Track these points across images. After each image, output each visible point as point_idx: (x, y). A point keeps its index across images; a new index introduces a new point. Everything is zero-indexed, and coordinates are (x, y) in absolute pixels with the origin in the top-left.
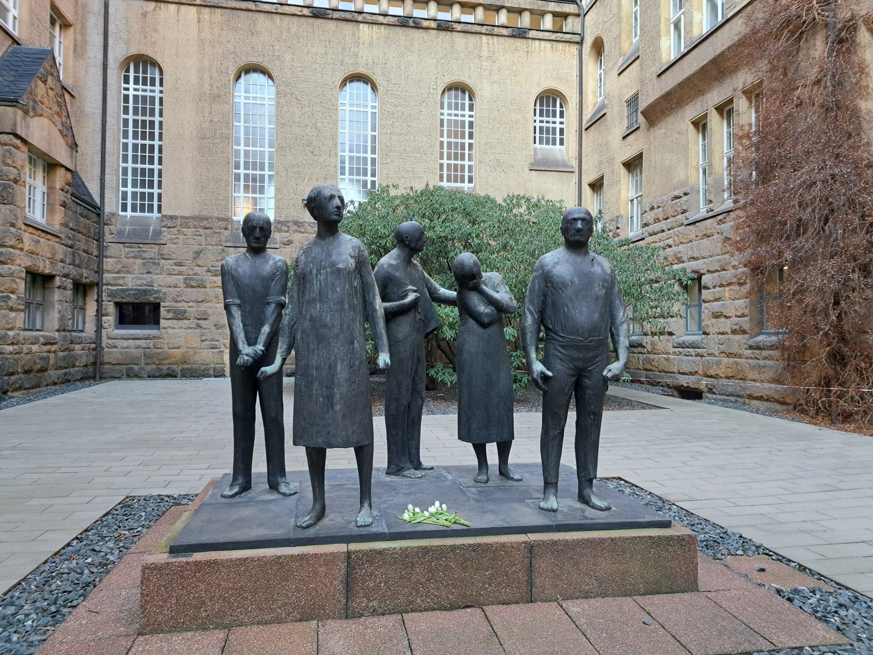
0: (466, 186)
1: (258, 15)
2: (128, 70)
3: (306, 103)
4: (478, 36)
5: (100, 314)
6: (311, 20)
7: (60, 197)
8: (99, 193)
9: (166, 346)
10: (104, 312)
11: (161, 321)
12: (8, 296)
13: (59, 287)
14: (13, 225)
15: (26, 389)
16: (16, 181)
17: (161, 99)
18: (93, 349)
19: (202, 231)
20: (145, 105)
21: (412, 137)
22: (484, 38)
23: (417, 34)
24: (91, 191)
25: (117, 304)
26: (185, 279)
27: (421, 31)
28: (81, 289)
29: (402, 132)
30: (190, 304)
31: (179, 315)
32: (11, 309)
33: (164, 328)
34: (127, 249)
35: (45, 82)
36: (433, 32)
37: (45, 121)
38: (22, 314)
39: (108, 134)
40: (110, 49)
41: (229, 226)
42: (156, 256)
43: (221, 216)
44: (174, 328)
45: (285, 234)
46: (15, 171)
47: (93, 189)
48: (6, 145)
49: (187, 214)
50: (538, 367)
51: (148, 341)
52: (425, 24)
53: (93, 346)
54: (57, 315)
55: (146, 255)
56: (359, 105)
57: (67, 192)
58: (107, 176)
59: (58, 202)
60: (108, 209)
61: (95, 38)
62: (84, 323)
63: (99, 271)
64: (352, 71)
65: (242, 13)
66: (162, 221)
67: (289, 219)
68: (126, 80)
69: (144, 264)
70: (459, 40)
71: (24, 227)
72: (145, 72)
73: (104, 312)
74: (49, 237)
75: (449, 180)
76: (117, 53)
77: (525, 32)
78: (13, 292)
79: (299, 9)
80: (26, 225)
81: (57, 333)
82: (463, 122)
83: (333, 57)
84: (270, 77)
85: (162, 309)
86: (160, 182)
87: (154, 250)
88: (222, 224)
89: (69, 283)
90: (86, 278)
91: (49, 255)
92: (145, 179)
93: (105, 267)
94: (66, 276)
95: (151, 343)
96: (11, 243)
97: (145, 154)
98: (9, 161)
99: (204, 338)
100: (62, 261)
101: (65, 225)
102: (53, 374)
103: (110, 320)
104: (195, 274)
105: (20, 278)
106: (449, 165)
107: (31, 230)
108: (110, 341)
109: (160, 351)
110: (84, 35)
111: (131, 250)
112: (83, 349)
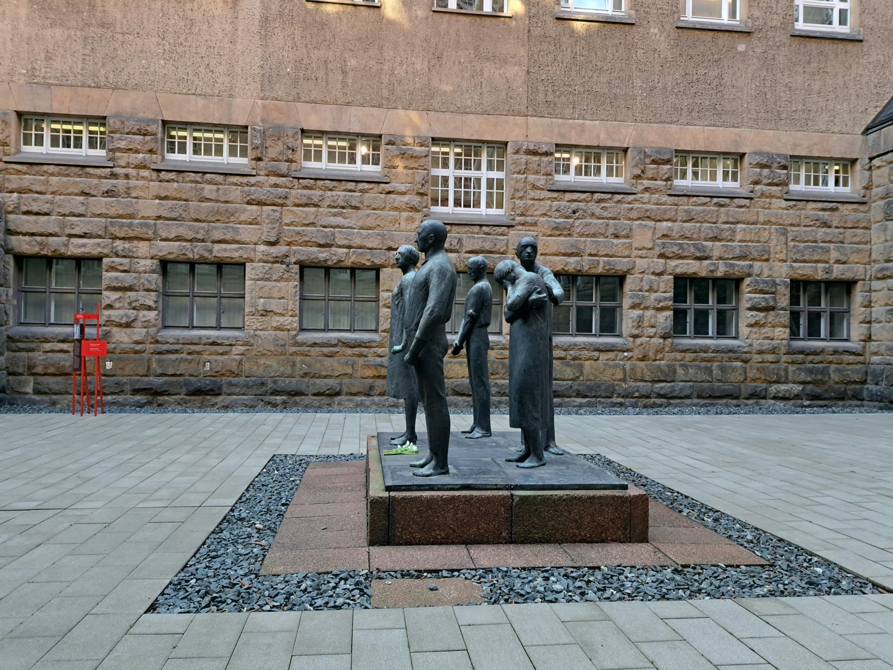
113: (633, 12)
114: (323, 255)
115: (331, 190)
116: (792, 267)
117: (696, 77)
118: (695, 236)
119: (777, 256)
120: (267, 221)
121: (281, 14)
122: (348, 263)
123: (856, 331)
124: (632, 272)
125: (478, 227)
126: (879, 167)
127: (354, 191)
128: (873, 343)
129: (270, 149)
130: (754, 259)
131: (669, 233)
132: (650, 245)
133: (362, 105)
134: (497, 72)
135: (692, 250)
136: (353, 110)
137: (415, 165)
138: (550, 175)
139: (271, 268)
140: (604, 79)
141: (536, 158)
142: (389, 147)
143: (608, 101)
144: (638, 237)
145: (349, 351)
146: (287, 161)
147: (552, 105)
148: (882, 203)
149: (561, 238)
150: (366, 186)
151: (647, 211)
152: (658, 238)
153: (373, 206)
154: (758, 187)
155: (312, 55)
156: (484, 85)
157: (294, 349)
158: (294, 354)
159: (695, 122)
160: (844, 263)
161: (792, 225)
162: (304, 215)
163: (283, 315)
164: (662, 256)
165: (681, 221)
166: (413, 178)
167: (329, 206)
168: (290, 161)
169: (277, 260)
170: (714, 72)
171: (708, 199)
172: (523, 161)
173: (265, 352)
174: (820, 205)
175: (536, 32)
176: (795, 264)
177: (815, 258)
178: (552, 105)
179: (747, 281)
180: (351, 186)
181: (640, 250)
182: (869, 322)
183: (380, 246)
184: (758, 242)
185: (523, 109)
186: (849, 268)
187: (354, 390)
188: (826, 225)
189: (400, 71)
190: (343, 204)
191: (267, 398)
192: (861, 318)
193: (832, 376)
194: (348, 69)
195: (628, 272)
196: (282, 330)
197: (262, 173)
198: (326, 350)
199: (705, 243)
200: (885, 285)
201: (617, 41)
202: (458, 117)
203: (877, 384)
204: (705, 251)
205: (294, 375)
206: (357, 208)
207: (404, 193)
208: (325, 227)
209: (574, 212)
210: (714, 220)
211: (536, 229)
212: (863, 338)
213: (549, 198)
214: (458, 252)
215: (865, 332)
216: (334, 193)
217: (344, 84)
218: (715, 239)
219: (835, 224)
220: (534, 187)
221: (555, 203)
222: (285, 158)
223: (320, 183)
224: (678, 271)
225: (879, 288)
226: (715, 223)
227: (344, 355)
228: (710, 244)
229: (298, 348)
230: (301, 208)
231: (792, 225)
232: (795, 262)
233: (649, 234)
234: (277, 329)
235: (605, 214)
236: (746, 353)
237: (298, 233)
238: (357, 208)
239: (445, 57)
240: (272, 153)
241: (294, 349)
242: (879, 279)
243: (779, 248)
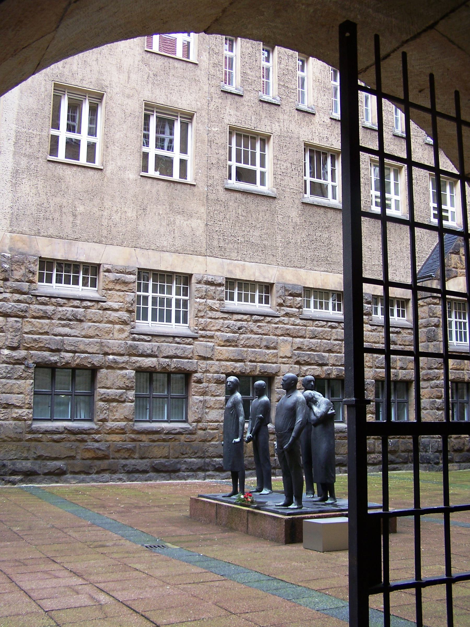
12: (435, 401)
15: (457, 462)
48: (430, 304)
50: (275, 443)
96: (435, 366)
113: (275, 189)
114: (54, 358)
115: (61, 306)
116: (375, 371)
117: (315, 237)
118: (317, 349)
120: (11, 330)
121: (28, 168)
122: (73, 365)
124: (279, 374)
125: (172, 338)
126: (422, 306)
127: (79, 307)
129: (15, 272)
131: (302, 346)
132: (289, 355)
133: (87, 241)
134: (185, 223)
135: (316, 359)
136: (80, 244)
137: (126, 289)
138: (223, 300)
139: (12, 369)
140: (257, 233)
141: (213, 288)
142: (107, 274)
143: (260, 249)
144: (282, 349)
145: (73, 437)
146: (27, 282)
147: (223, 250)
149: (231, 348)
150: (89, 304)
151: (287, 329)
152: (295, 350)
153: (94, 319)
155: (50, 201)
156: (176, 231)
157: (29, 436)
158: (30, 440)
159: (315, 268)
160: (405, 369)
162: (40, 326)
163: (20, 407)
164: (298, 363)
165: (309, 338)
166: (124, 299)
167: (60, 319)
168: (31, 282)
169: (19, 362)
170: (326, 235)
171: (325, 323)
172: (204, 289)
173: (6, 438)
175: (212, 197)
178: (223, 250)
180: (77, 303)
181: (283, 358)
183: (98, 352)
185: (203, 250)
186: (408, 372)
187: (77, 470)
189: (116, 217)
190: (71, 317)
191: (8, 478)
193: (400, 447)
194: (77, 213)
195: (276, 374)
196: (20, 420)
197: (8, 291)
198: (56, 437)
199: (324, 354)
200: (429, 385)
201: (265, 208)
202: (157, 254)
204: (324, 360)
205: (29, 457)
206: (81, 321)
207: (117, 310)
208: (56, 335)
209: (239, 329)
210: (329, 338)
211: (213, 340)
213: (222, 318)
214: (156, 356)
216: (64, 308)
217: (74, 225)
218: (330, 351)
219: (399, 342)
220: (212, 309)
221: (226, 322)
222: (26, 279)
223: (53, 300)
225: (425, 386)
226: (329, 340)
227: (69, 441)
228: (326, 354)
229: (33, 436)
230: (37, 320)
232: (377, 368)
233: (289, 347)
234: (15, 419)
235: (260, 331)
237: (35, 340)
238: (81, 321)
239: (148, 209)
240: (17, 275)
241: (29, 436)
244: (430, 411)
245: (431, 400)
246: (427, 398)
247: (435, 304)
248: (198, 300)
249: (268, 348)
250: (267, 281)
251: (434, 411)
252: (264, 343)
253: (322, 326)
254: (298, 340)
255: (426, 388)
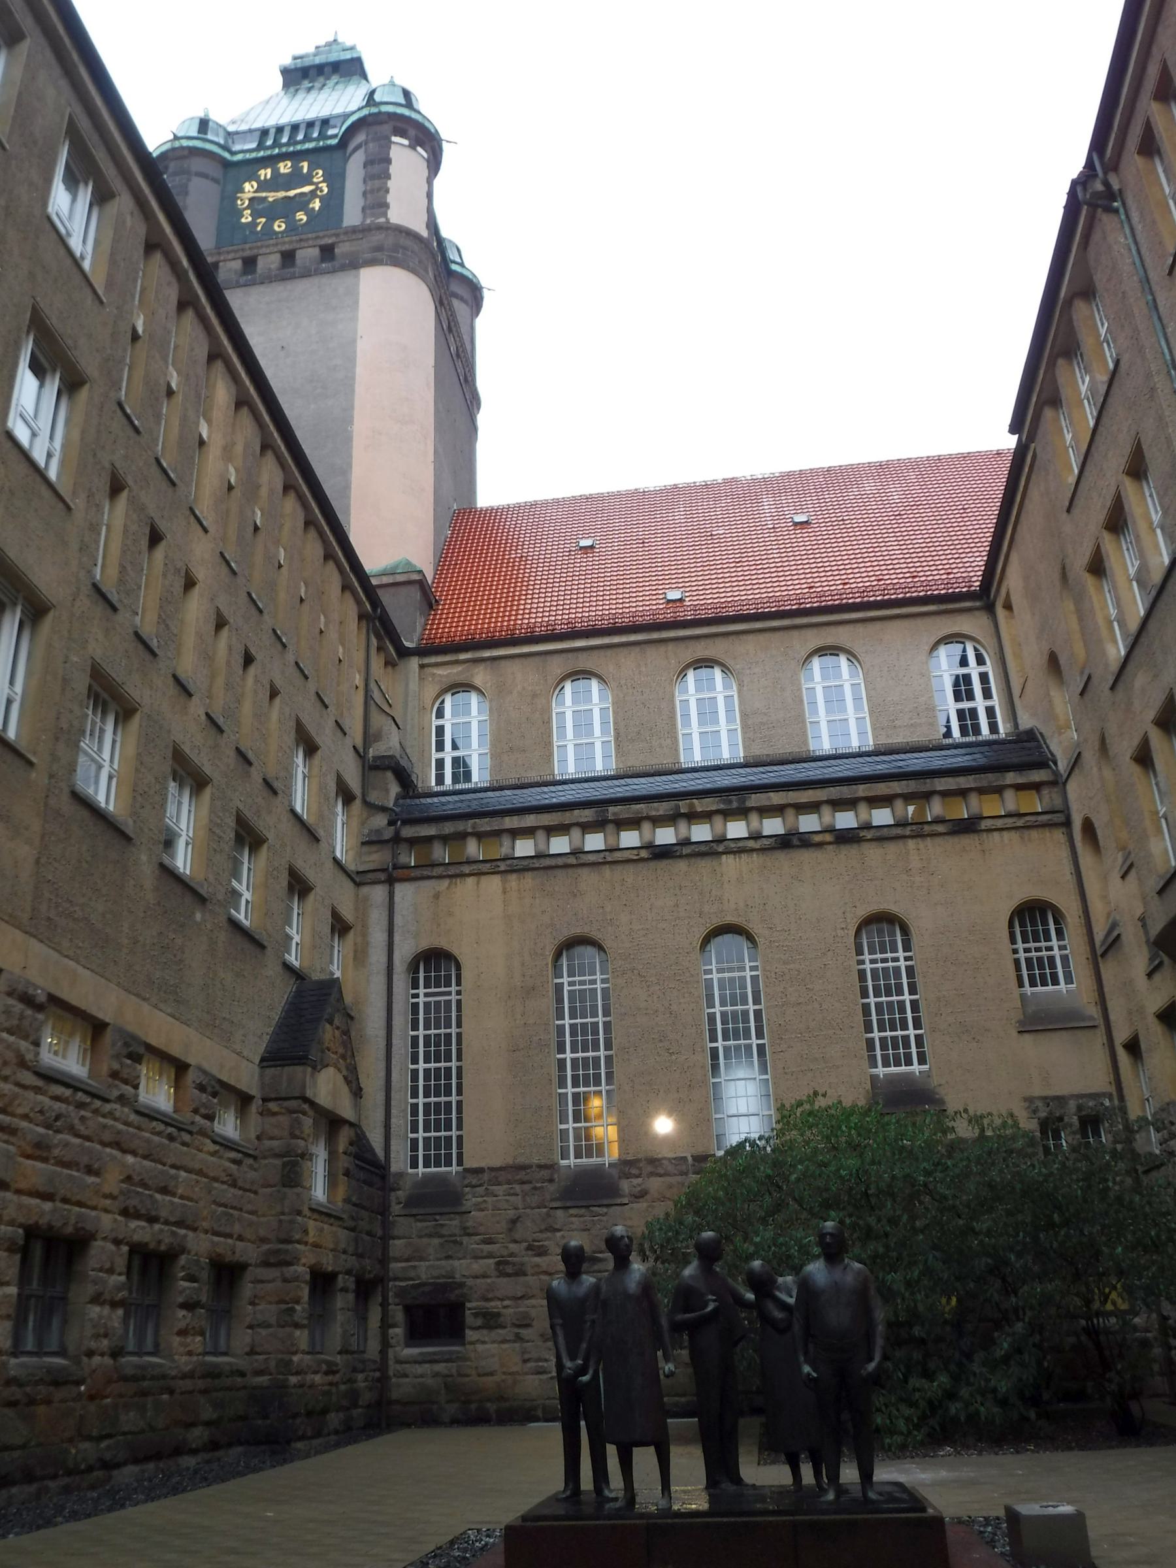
0: (916, 1068)
1: (580, 871)
2: (417, 971)
3: (653, 979)
4: (900, 843)
5: (385, 1325)
6: (652, 864)
7: (344, 1162)
8: (382, 1145)
9: (474, 1372)
10: (390, 1321)
11: (467, 1331)
13: (342, 1290)
14: (299, 1213)
16: (303, 1156)
17: (459, 1002)
18: (379, 1380)
19: (518, 1188)
20: (438, 1014)
21: (816, 1005)
22: (911, 843)
23: (806, 855)
24: (374, 1144)
25: (408, 1310)
26: (498, 1264)
27: (811, 850)
28: (366, 1289)
29: (801, 1000)
30: (506, 1303)
31: (491, 1321)
32: (297, 1326)
33: (471, 1343)
34: (419, 1224)
35: (331, 1023)
36: (831, 847)
37: (331, 1070)
38: (306, 1332)
39: (394, 1062)
40: (395, 947)
41: (556, 1176)
42: (457, 1231)
43: (543, 1162)
44: (484, 1342)
45: (640, 1180)
46: (301, 1143)
47: (376, 1139)
48: (295, 1112)
49: (497, 1163)
51: (450, 1365)
52: (817, 838)
53: (377, 1374)
54: (339, 1330)
55: (444, 1231)
56: (730, 970)
57: (350, 1155)
58: (393, 1120)
59: (341, 1172)
60: (394, 1168)
61: (378, 937)
62: (366, 1339)
63: (384, 1261)
64: (716, 921)
65: (559, 872)
66: (464, 1178)
67: (639, 1156)
68: (415, 985)
69: (441, 1245)
70: (873, 853)
71: (308, 1213)
72: (438, 970)
73: (390, 1321)
74: (332, 1220)
75: (886, 1064)
76: (405, 950)
77: (973, 824)
78: (298, 1302)
79: (635, 852)
80: (311, 1209)
81: (339, 1357)
82: (897, 970)
83: (687, 907)
84: (601, 948)
85: (468, 1312)
86: (460, 1120)
87: (454, 1223)
88: (545, 1173)
89: (351, 1283)
90: (370, 1272)
91: (332, 1246)
92: (439, 1117)
93: (391, 1254)
94: (349, 1272)
95: (453, 1367)
96: (297, 1237)
97: (439, 1083)
98: (297, 1133)
99: (526, 1356)
100: (345, 1252)
101: (347, 1201)
102: (334, 1419)
103: (398, 1332)
104: (512, 1255)
105: (305, 1282)
106: (883, 1040)
107: (316, 1216)
108: (398, 1367)
109: (467, 1379)
110: (364, 935)
111: (425, 1224)
112: (366, 1380)
119: (204, 1224)
123: (242, 1339)
126: (274, 1114)
128: (257, 1357)
130: (188, 1227)
132: (116, 1192)
148: (278, 1162)
151: (119, 1132)
154: (198, 1118)
160: (242, 1240)
161: (215, 1179)
164: (125, 1212)
174: (233, 1155)
176: (216, 1239)
177: (228, 1230)
179: (183, 1260)
182: (250, 1327)
184: (191, 1200)
188: (234, 1184)
192: (248, 1320)
203: (266, 1417)
209: (57, 1118)
212: (247, 1349)
215: (248, 1340)
218: (164, 1190)
219: (240, 1183)
224: (136, 1238)
228: (158, 1196)
231: (215, 1179)
235: (81, 1128)
236: (174, 1378)
242: (266, 1264)
243: (205, 1212)
244: (280, 1330)
245: (284, 1306)
246: (270, 1303)
247: (304, 1113)
248: (5, 1035)
249: (90, 1171)
250: (100, 1015)
251: (288, 1329)
252: (85, 1160)
253: (159, 1134)
254: (130, 1159)
255: (269, 1282)
